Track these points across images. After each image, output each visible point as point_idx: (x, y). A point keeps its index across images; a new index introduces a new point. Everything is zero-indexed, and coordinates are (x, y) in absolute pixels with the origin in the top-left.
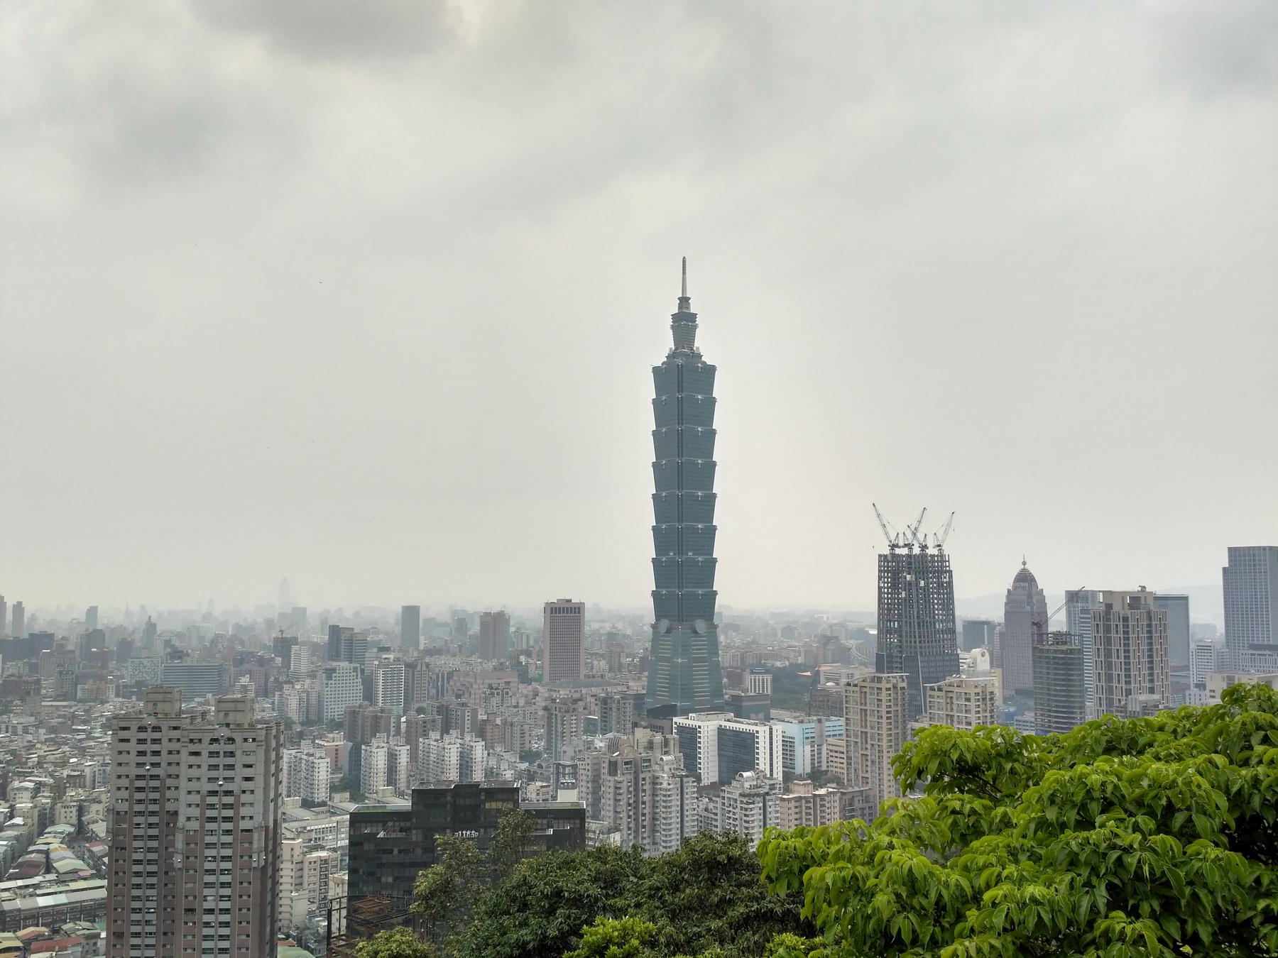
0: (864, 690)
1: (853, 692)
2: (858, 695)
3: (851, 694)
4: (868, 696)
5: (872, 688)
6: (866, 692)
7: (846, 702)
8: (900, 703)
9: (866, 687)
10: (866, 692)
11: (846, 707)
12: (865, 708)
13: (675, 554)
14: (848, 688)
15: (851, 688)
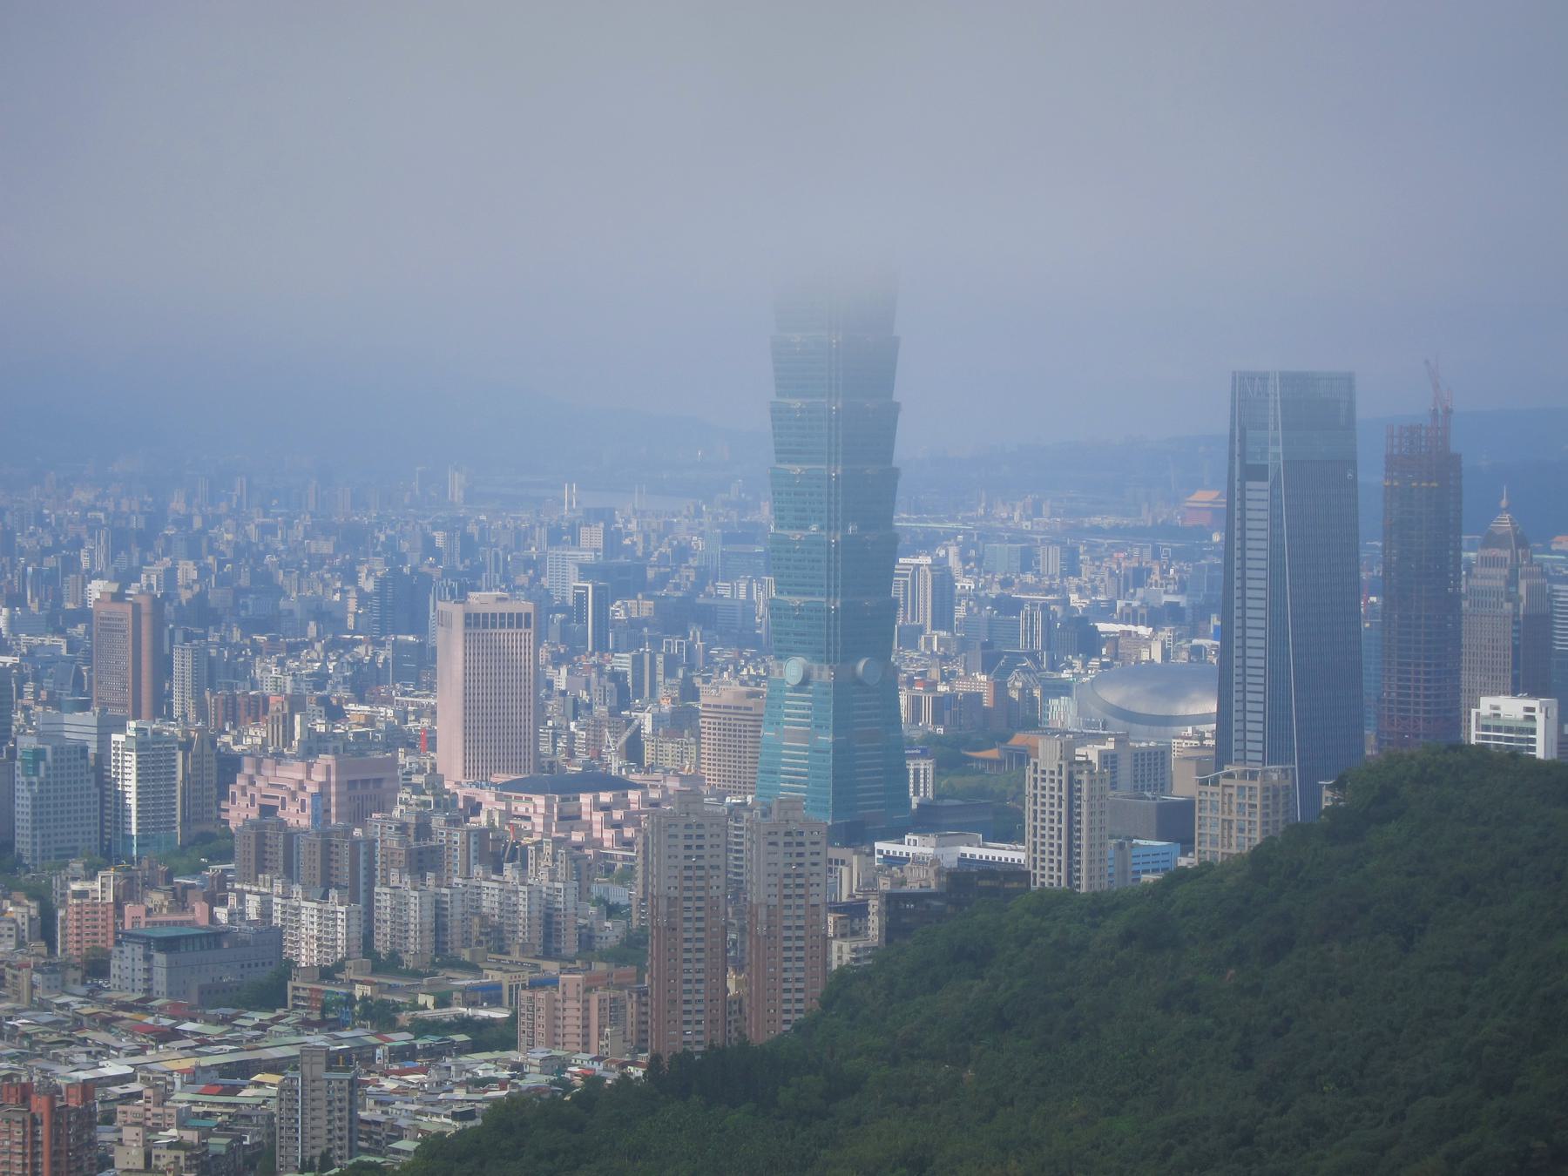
0: (1228, 791)
1: (1212, 794)
2: (1219, 798)
3: (1209, 797)
4: (1235, 800)
5: (1241, 788)
6: (1231, 795)
7: (1200, 810)
8: (1281, 810)
9: (1231, 786)
10: (1231, 795)
11: (1200, 818)
12: (1229, 818)
13: (822, 528)
14: (1203, 788)
15: (1210, 789)
